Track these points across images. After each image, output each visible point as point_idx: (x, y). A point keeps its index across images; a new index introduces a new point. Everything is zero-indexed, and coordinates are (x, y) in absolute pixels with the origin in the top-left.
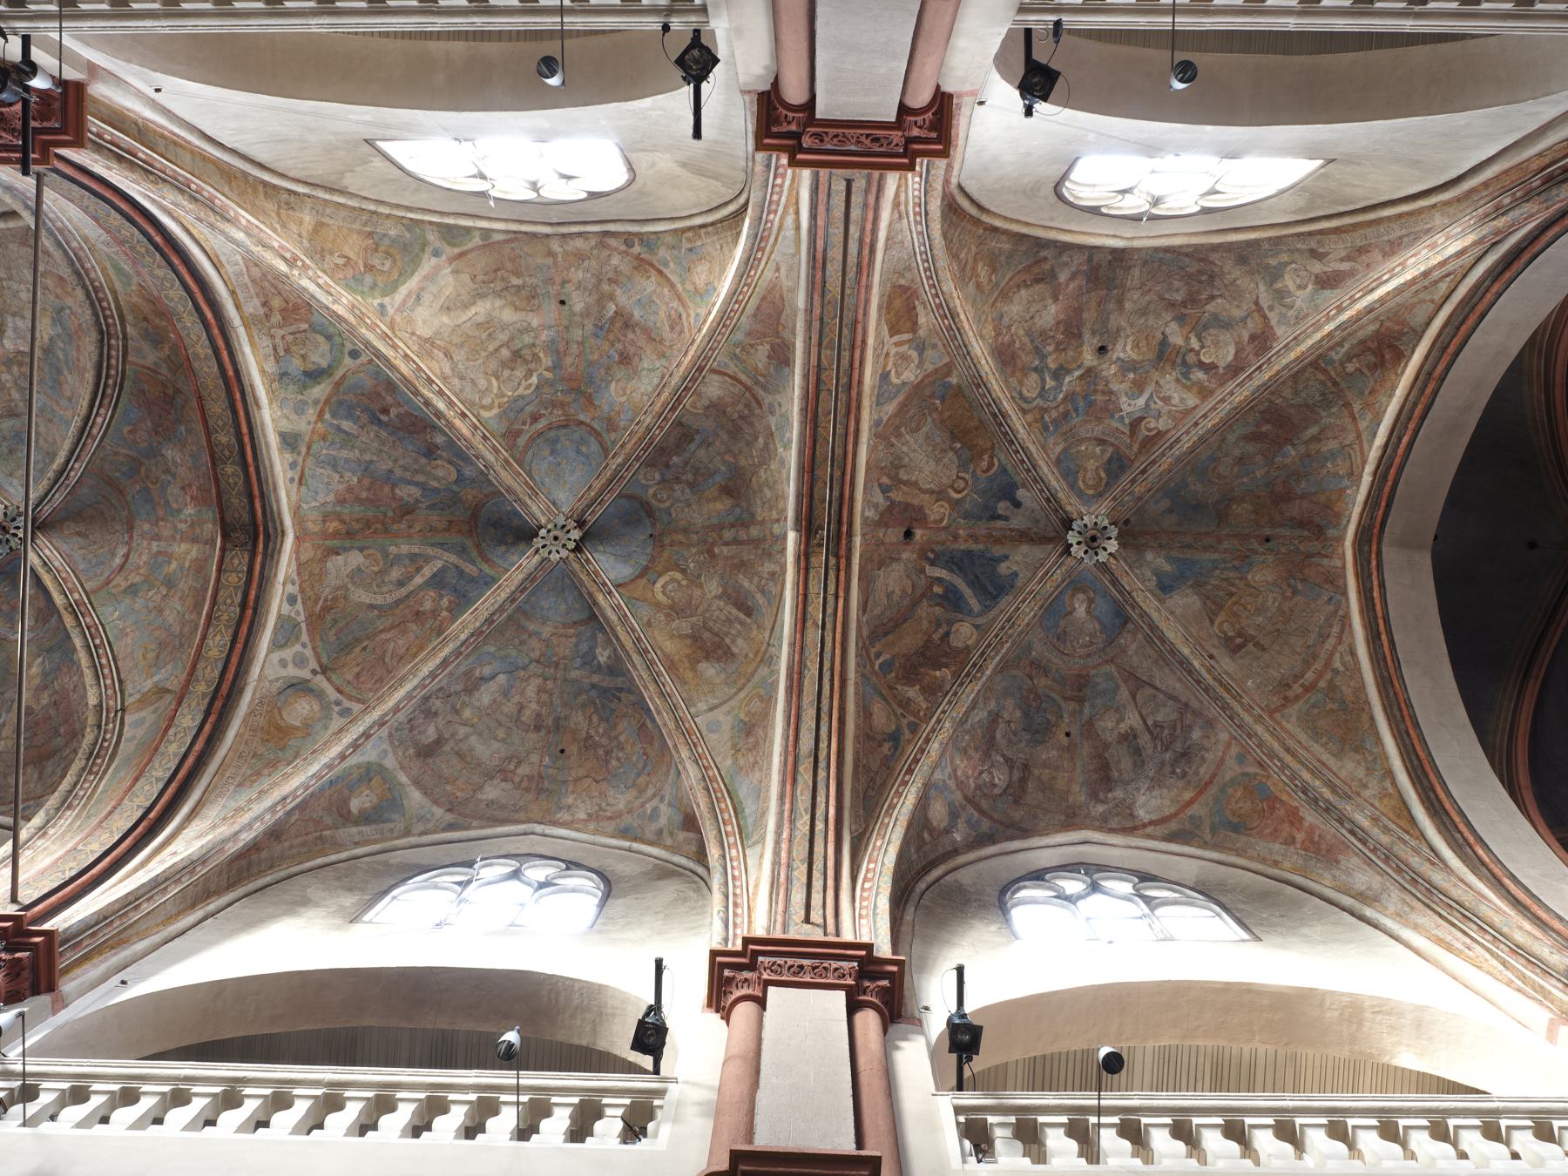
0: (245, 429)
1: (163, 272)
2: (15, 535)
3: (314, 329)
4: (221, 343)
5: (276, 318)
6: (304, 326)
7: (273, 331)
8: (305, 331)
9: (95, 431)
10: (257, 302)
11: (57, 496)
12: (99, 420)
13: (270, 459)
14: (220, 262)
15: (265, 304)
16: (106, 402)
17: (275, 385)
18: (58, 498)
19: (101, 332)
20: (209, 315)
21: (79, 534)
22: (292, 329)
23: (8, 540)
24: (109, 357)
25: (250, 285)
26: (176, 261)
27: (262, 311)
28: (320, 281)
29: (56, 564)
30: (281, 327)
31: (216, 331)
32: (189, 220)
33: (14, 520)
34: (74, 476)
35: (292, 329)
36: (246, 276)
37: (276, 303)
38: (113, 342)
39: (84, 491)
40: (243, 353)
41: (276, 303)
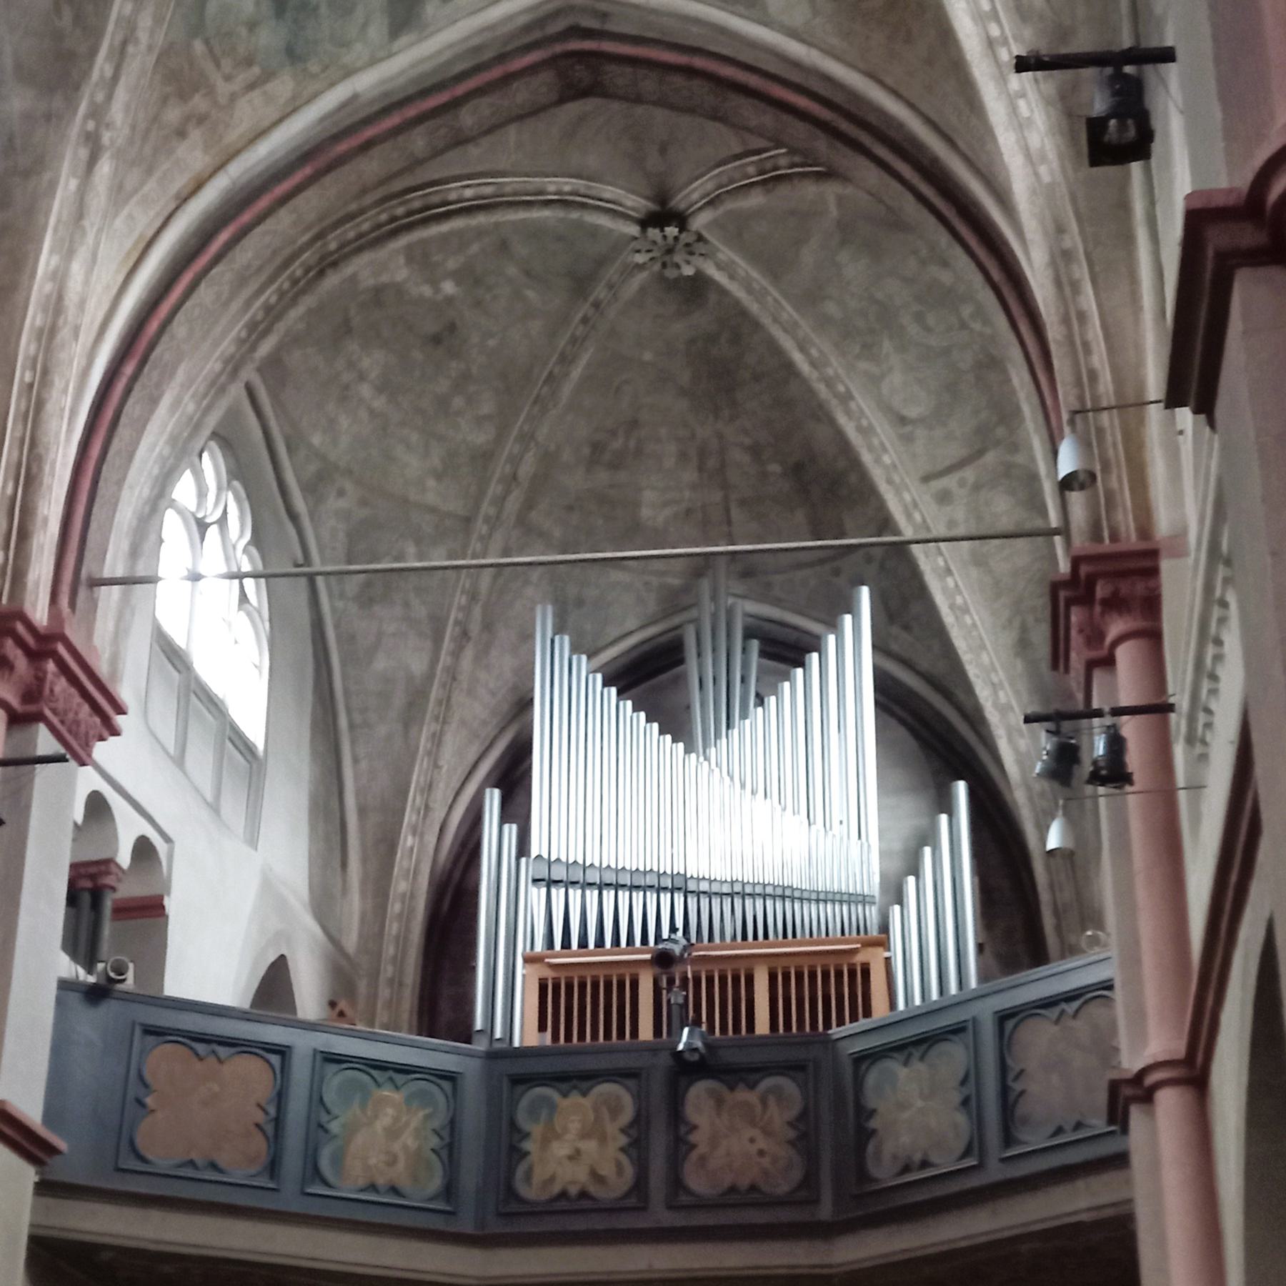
0: (394, 120)
1: (179, 328)
2: (676, 238)
3: (197, 28)
4: (263, 203)
5: (199, 103)
6: (198, 46)
7: (222, 100)
8: (207, 42)
9: (488, 190)
10: (182, 150)
11: (607, 195)
12: (468, 193)
13: (439, 52)
14: (137, 243)
15: (181, 134)
16: (436, 199)
17: (314, 67)
18: (609, 192)
19: (321, 273)
20: (224, 237)
21: (663, 150)
22: (209, 67)
23: (687, 245)
24: (360, 236)
25: (158, 174)
26: (153, 326)
27: (195, 135)
28: (109, 72)
29: (710, 186)
30: (211, 92)
31: (246, 217)
32: (86, 337)
33: (654, 243)
34: (568, 184)
35: (209, 67)
36: (146, 189)
37: (173, 115)
38: (333, 246)
39: (592, 162)
40: (271, 153)
41: (173, 115)
